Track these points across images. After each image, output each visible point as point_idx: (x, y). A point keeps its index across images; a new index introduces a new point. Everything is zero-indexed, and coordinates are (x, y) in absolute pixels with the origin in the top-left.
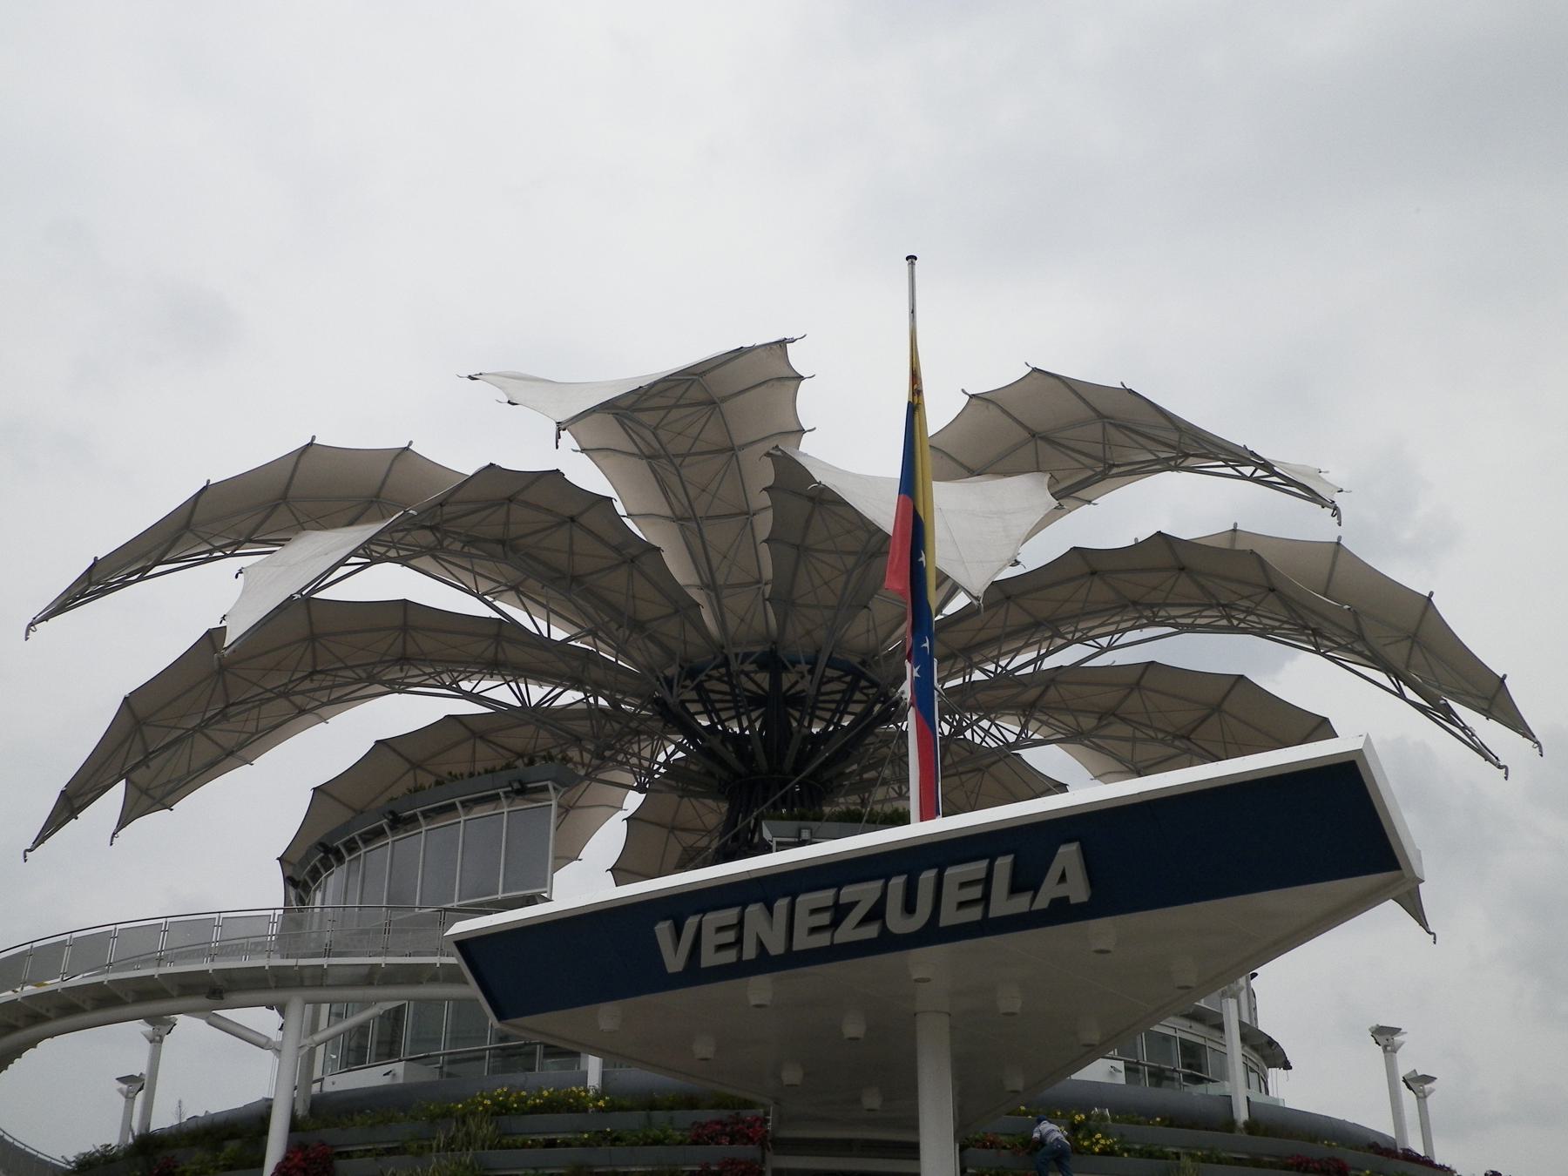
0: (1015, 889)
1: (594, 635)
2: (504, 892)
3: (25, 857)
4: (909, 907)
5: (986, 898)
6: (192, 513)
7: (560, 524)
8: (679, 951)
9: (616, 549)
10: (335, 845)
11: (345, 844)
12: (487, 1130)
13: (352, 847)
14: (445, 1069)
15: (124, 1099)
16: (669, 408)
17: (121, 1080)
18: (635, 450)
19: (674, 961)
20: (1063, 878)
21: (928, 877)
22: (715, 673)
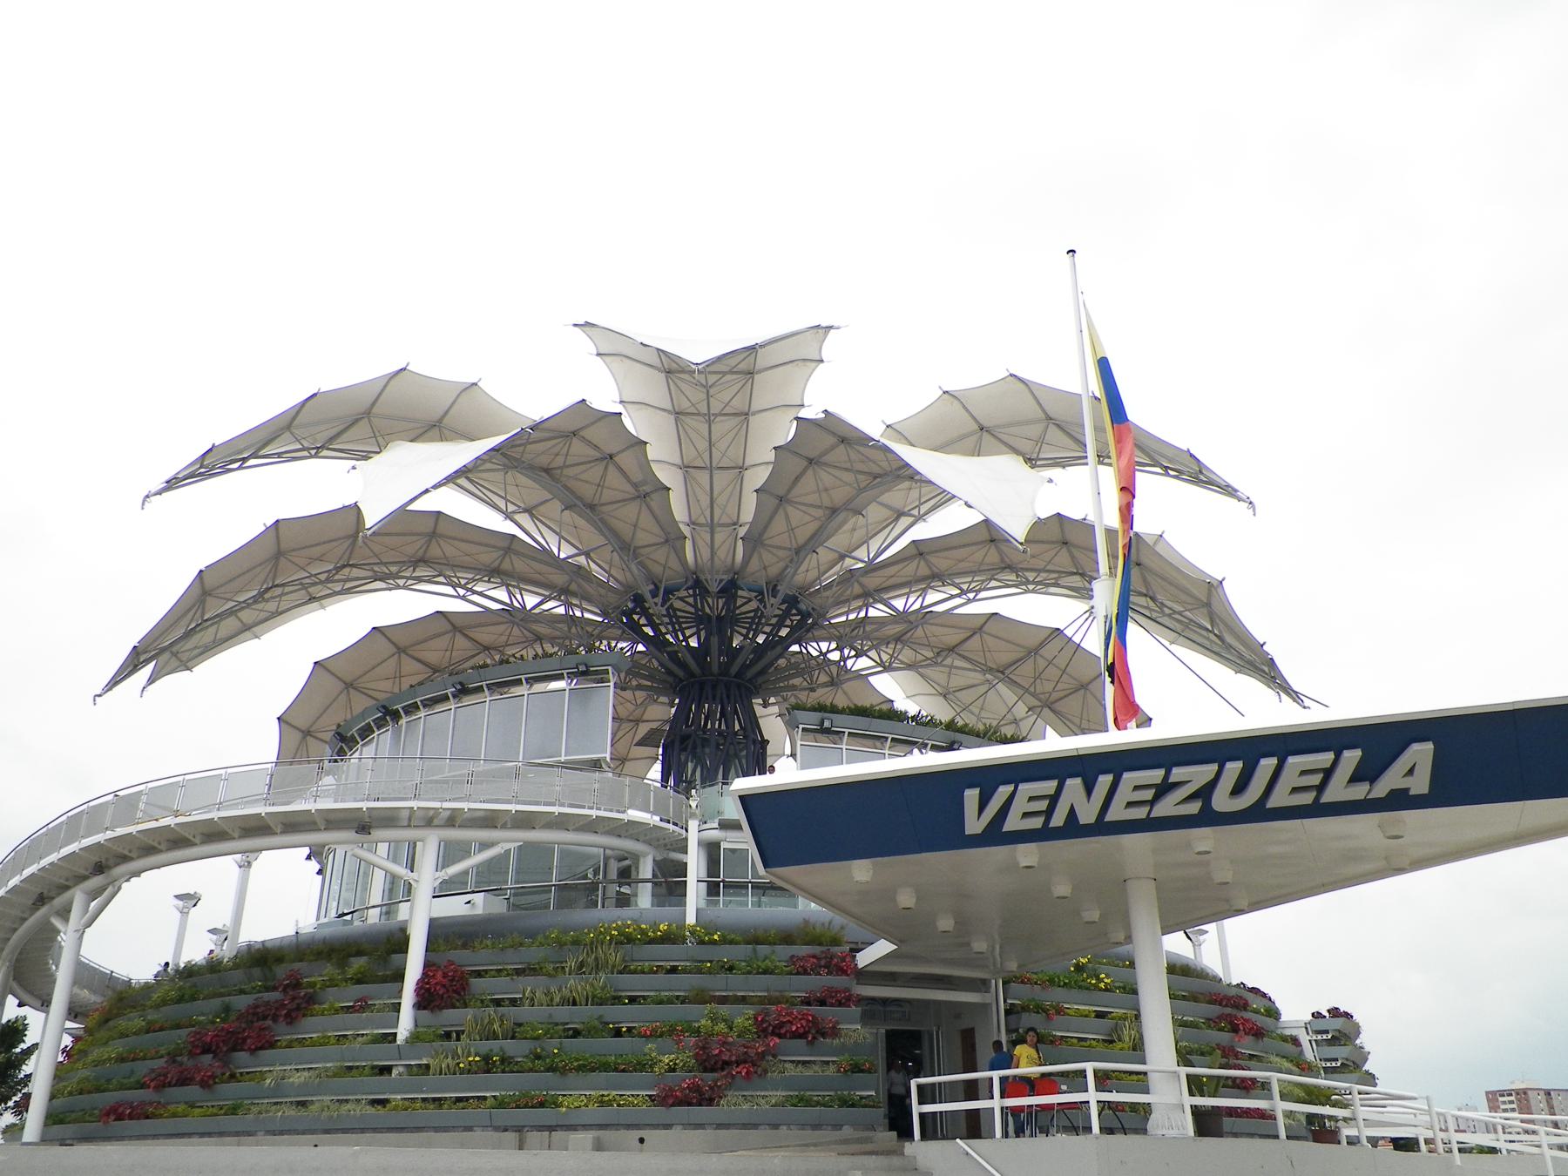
0: (1355, 779)
1: (587, 555)
2: (565, 756)
3: (94, 701)
4: (1239, 788)
5: (1321, 788)
6: (298, 413)
7: (602, 459)
9: (635, 485)
13: (411, 709)
14: (511, 900)
15: (180, 914)
16: (724, 374)
18: (670, 408)
19: (974, 824)
20: (1411, 772)
21: (1271, 762)
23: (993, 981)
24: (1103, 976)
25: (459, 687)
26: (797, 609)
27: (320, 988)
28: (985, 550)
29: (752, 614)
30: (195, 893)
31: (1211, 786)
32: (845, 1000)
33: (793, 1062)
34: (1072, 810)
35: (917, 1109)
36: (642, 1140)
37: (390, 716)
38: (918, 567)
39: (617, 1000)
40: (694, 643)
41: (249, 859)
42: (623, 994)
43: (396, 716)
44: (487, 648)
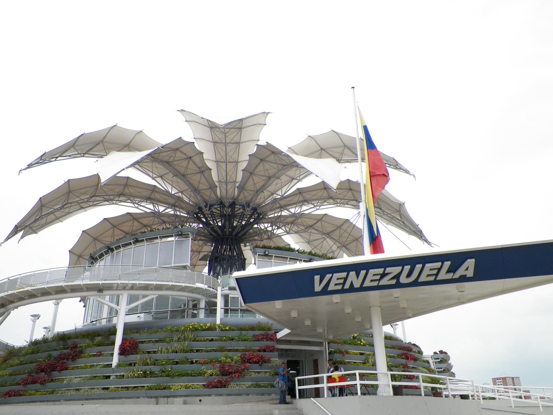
0: (448, 271)
1: (182, 193)
3: (1, 245)
4: (409, 275)
5: (437, 275)
6: (76, 142)
7: (188, 158)
8: (320, 286)
9: (199, 168)
10: (112, 247)
11: (115, 247)
12: (191, 336)
13: (118, 248)
14: (154, 316)
16: (231, 128)
17: (32, 316)
19: (318, 288)
20: (467, 269)
21: (420, 266)
22: (216, 206)
23: (324, 343)
24: (362, 340)
25: (135, 240)
26: (257, 212)
27: (84, 348)
28: (323, 191)
29: (241, 214)
30: (38, 314)
31: (399, 274)
32: (272, 350)
33: (254, 372)
34: (352, 283)
35: (297, 388)
36: (200, 401)
37: (110, 250)
38: (299, 197)
39: (192, 351)
40: (220, 224)
41: (58, 302)
42: (194, 349)
43: (112, 250)
44: (145, 226)
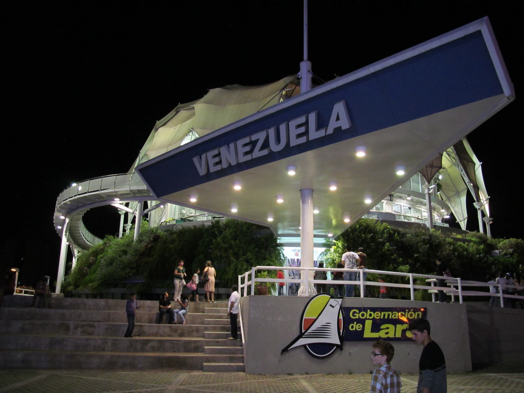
4: (278, 141)
5: (306, 133)
8: (202, 166)
20: (338, 119)
